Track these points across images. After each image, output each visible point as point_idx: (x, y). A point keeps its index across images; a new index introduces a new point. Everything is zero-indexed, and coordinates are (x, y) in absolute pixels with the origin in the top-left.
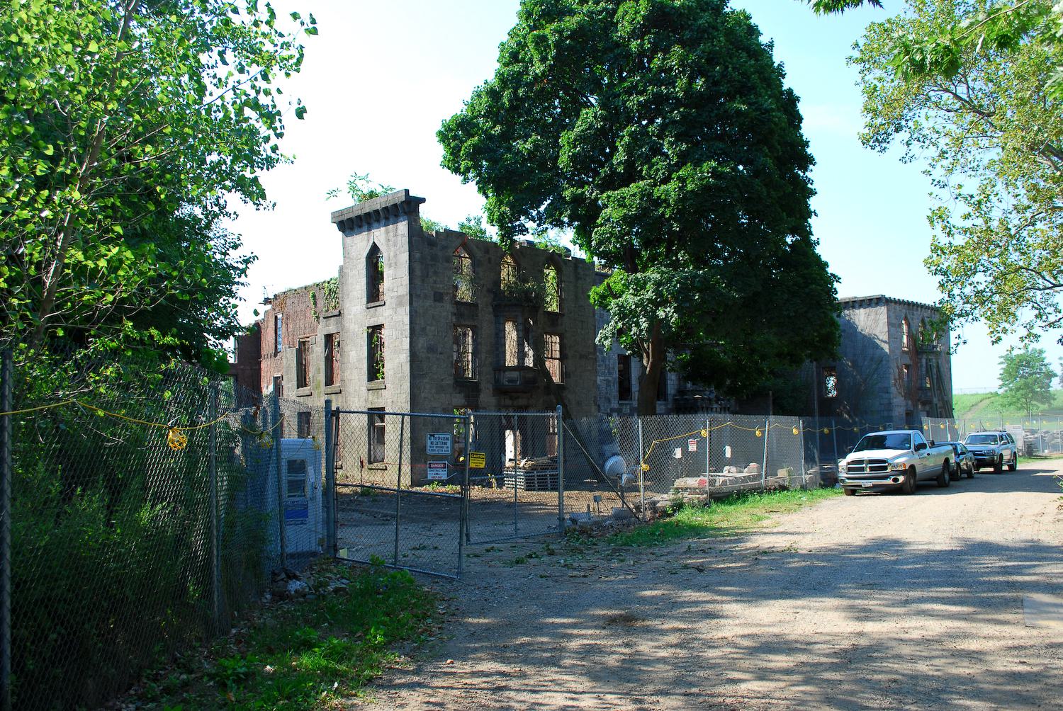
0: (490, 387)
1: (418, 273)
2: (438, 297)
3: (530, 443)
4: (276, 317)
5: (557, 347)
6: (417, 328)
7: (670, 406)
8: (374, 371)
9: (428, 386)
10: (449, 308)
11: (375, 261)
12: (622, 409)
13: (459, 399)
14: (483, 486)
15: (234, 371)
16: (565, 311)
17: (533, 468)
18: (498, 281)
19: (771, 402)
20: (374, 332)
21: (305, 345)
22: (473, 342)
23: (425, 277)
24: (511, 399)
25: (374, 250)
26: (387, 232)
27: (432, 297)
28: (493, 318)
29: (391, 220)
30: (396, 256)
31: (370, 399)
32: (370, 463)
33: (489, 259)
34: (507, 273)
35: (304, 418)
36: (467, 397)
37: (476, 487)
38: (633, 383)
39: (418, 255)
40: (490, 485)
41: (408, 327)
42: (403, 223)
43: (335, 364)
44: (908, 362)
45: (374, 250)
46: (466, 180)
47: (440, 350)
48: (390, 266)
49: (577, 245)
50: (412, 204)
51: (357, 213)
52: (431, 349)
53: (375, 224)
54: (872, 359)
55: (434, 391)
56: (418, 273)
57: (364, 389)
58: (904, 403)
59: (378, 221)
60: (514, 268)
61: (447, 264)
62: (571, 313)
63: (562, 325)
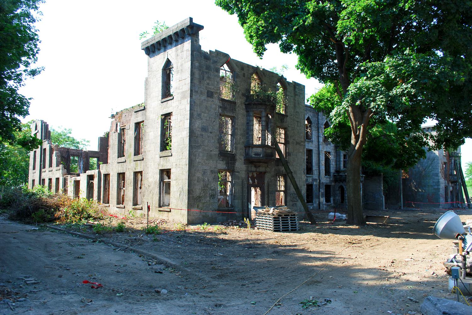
0: (243, 158)
1: (197, 76)
2: (210, 94)
3: (266, 196)
4: (117, 124)
5: (283, 136)
6: (195, 114)
7: (331, 179)
8: (165, 145)
9: (201, 155)
11: (168, 72)
12: (307, 179)
13: (222, 165)
14: (240, 227)
15: (97, 155)
16: (288, 114)
18: (249, 90)
19: (382, 179)
20: (166, 117)
21: (124, 131)
22: (232, 127)
23: (201, 80)
24: (255, 166)
25: (168, 63)
26: (177, 50)
27: (206, 94)
28: (245, 113)
29: (180, 41)
30: (182, 65)
31: (161, 163)
32: (160, 206)
33: (244, 75)
34: (254, 85)
35: (121, 176)
36: (227, 164)
37: (235, 227)
38: (313, 165)
40: (245, 226)
41: (189, 112)
42: (188, 42)
43: (142, 143)
44: (446, 161)
45: (168, 63)
47: (210, 130)
48: (178, 72)
49: (300, 70)
50: (195, 28)
52: (204, 129)
53: (169, 46)
54: (429, 159)
55: (205, 158)
56: (197, 76)
57: (158, 156)
58: (444, 182)
59: (171, 44)
60: (258, 84)
61: (216, 73)
62: (291, 115)
63: (286, 122)
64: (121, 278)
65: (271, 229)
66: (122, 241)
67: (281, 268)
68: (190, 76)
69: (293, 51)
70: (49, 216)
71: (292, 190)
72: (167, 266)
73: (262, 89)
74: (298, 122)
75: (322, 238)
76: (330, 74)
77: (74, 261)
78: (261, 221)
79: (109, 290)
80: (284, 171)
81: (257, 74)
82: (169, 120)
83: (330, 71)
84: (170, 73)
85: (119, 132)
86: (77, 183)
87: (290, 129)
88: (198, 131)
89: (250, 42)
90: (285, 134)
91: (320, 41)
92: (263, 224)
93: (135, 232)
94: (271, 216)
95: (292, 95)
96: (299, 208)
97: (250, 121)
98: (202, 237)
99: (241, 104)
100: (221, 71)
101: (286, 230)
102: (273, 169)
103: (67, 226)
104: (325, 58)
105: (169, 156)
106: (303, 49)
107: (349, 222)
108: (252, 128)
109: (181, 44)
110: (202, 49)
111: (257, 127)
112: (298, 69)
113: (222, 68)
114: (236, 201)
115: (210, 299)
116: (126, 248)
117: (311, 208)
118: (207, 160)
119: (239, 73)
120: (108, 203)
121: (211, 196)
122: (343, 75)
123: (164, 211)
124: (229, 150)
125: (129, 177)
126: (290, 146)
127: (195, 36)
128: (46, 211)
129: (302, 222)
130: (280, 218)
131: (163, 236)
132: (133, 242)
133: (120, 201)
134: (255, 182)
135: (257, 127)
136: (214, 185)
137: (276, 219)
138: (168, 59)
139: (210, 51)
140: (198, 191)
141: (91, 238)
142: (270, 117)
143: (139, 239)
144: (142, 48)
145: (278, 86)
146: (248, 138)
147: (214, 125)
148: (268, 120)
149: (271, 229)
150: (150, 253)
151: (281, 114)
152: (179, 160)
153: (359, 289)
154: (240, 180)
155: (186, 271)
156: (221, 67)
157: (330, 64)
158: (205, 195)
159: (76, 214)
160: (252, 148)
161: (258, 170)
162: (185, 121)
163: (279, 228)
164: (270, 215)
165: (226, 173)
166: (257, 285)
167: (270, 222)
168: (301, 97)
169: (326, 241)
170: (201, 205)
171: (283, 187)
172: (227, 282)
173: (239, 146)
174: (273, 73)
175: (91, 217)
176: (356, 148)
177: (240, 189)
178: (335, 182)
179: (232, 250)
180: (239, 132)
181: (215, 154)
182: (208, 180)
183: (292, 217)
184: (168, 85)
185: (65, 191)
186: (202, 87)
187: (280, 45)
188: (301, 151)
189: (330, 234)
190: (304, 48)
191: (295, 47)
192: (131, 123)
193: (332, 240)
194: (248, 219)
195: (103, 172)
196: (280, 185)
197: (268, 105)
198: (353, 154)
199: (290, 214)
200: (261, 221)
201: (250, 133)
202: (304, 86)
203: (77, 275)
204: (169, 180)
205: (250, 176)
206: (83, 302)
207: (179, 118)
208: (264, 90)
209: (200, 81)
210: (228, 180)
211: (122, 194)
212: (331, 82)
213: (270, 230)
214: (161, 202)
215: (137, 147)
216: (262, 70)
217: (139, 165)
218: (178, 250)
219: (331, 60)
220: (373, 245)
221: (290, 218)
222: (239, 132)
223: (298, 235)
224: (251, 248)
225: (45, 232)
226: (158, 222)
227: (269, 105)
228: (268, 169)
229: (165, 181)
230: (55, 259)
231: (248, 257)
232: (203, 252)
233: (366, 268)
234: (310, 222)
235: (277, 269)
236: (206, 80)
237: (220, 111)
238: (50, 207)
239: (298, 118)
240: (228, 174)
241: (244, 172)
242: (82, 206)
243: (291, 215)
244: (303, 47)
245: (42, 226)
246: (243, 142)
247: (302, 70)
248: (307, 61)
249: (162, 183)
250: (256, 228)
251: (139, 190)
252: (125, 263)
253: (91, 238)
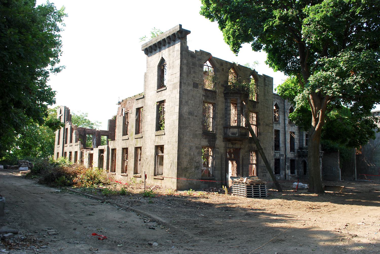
1: (185, 71)
3: (241, 168)
4: (122, 109)
5: (255, 119)
6: (184, 101)
7: (296, 155)
8: (159, 126)
9: (188, 134)
10: (201, 91)
11: (162, 68)
12: (276, 155)
13: (205, 142)
14: (219, 193)
15: (107, 134)
16: (259, 101)
17: (251, 184)
18: (227, 81)
19: (339, 155)
20: (161, 103)
21: (127, 115)
22: (213, 112)
23: (189, 73)
24: (232, 144)
25: (162, 61)
26: (169, 51)
27: (192, 85)
28: (224, 100)
29: (172, 44)
30: (173, 62)
31: (157, 140)
32: (155, 175)
33: (223, 69)
34: (231, 78)
35: (125, 150)
36: (209, 141)
37: (215, 193)
38: (281, 143)
39: (185, 62)
40: (223, 192)
43: (142, 125)
45: (163, 60)
46: (213, 21)
47: (195, 114)
48: (170, 68)
49: (268, 65)
50: (183, 33)
51: (155, 42)
52: (191, 113)
53: (163, 48)
55: (191, 136)
56: (185, 71)
57: (154, 135)
59: (165, 45)
60: (235, 77)
61: (201, 69)
62: (262, 102)
63: (257, 108)
64: (122, 232)
65: (244, 195)
66: (125, 202)
67: (252, 227)
68: (179, 71)
69: (263, 49)
70: (69, 181)
71: (263, 163)
72: (159, 223)
73: (237, 80)
74: (267, 107)
75: (287, 204)
76: (294, 68)
77: (86, 217)
78: (237, 189)
79: (112, 241)
80: (256, 147)
81: (234, 69)
82: (163, 106)
83: (293, 65)
84: (164, 69)
85: (124, 115)
86: (91, 156)
87: (260, 113)
88: (186, 115)
89: (228, 43)
90: (257, 117)
91: (285, 42)
92: (238, 191)
93: (134, 195)
94: (244, 185)
95: (263, 85)
96: (268, 178)
97: (228, 106)
98: (187, 201)
99: (221, 93)
100: (205, 67)
101: (256, 196)
102: (247, 147)
103: (82, 190)
104: (289, 55)
105: (163, 135)
106: (271, 48)
107: (310, 191)
108: (229, 113)
109: (172, 46)
110: (189, 49)
111: (233, 112)
112: (267, 64)
113: (205, 64)
114: (216, 172)
115: (192, 251)
116: (127, 208)
117: (279, 178)
118: (193, 138)
119: (219, 68)
120: (115, 172)
121: (196, 167)
122: (305, 69)
123: (158, 179)
124: (211, 130)
125: (131, 151)
126: (261, 127)
127: (184, 39)
128: (66, 177)
129: (271, 190)
130: (252, 186)
131: (156, 199)
132: (132, 203)
133: (124, 170)
134: (232, 157)
135: (233, 112)
136: (198, 158)
137: (249, 187)
138: (162, 57)
139: (196, 51)
140: (185, 163)
141: (100, 199)
142: (245, 104)
143: (138, 202)
144: (142, 49)
145: (250, 78)
146: (226, 120)
147: (199, 110)
148: (242, 107)
149: (244, 195)
150: (146, 213)
151: (253, 101)
152: (170, 138)
153: (316, 247)
154: (220, 155)
155: (174, 228)
156: (204, 63)
157: (294, 60)
158: (191, 166)
159: (89, 180)
160: (229, 129)
161: (234, 146)
162: (176, 107)
163: (251, 195)
164: (243, 183)
165: (208, 149)
166: (231, 241)
167: (244, 190)
168: (270, 87)
169: (291, 206)
170: (187, 175)
171: (255, 160)
172: (207, 238)
173: (219, 127)
174: (247, 68)
175: (101, 182)
176: (316, 129)
177: (219, 162)
178: (299, 157)
179: (212, 212)
180: (219, 116)
181: (200, 134)
182: (194, 154)
183: (262, 185)
184: (162, 78)
185: (82, 162)
186: (189, 79)
187: (252, 45)
188: (270, 131)
189: (294, 201)
190: (272, 47)
191: (264, 46)
192: (133, 109)
193: (295, 205)
194: (225, 187)
195: (111, 147)
196: (252, 159)
197: (242, 94)
198: (313, 134)
199: (260, 183)
200: (237, 189)
201: (228, 117)
202: (272, 78)
203: (88, 229)
204: (163, 154)
205: (228, 151)
206: (91, 250)
207: (170, 104)
208: (239, 81)
209: (188, 75)
210: (210, 154)
211: (126, 164)
212: (294, 74)
213: (244, 196)
214: (156, 172)
215: (137, 127)
216: (237, 65)
217: (139, 142)
218: (168, 211)
219: (294, 57)
220: (330, 210)
221: (261, 186)
222: (219, 116)
223: (267, 201)
224: (227, 210)
225: (65, 194)
226: (153, 188)
227: (244, 94)
228: (243, 146)
229: (159, 154)
230: (72, 215)
231: (225, 218)
232: (188, 213)
233: (323, 230)
234: (277, 190)
235: (248, 228)
236: (192, 74)
237: (204, 99)
238: (69, 174)
239: (267, 104)
240: (210, 149)
241: (223, 148)
242: (94, 174)
243: (262, 184)
244: (270, 46)
245: (63, 189)
246: (222, 124)
247: (271, 65)
248: (274, 58)
249: (157, 157)
250: (232, 194)
251: (139, 162)
252: (126, 220)
253: (100, 199)
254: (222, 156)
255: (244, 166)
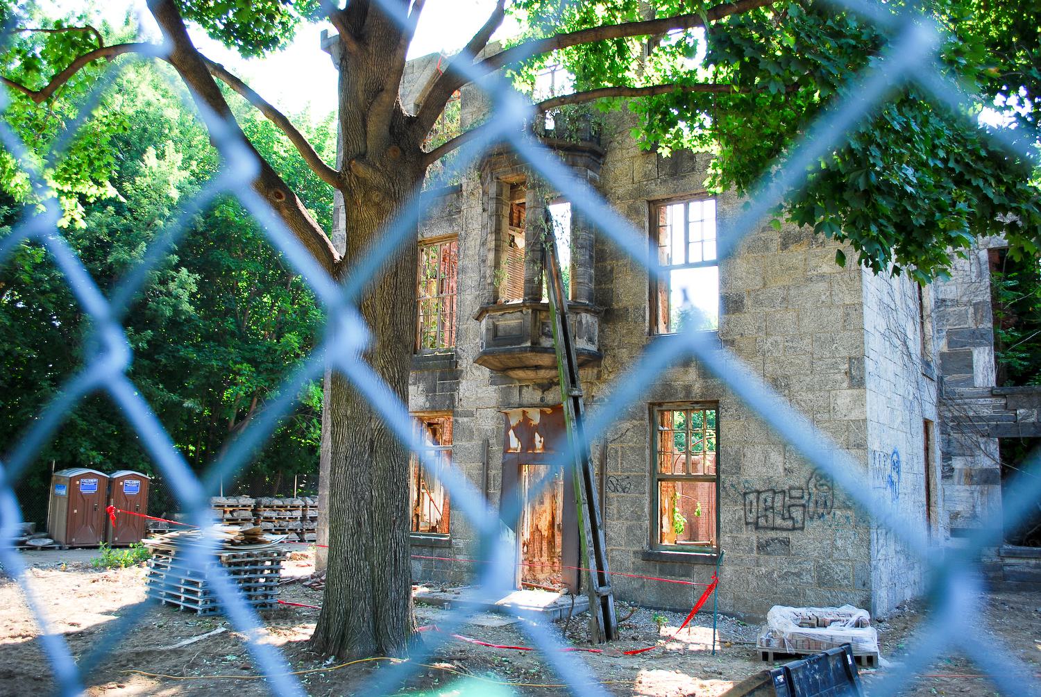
134: (534, 447)
154: (477, 442)
205: (514, 422)
241: (491, 412)
254: (486, 445)
255: (616, 490)
